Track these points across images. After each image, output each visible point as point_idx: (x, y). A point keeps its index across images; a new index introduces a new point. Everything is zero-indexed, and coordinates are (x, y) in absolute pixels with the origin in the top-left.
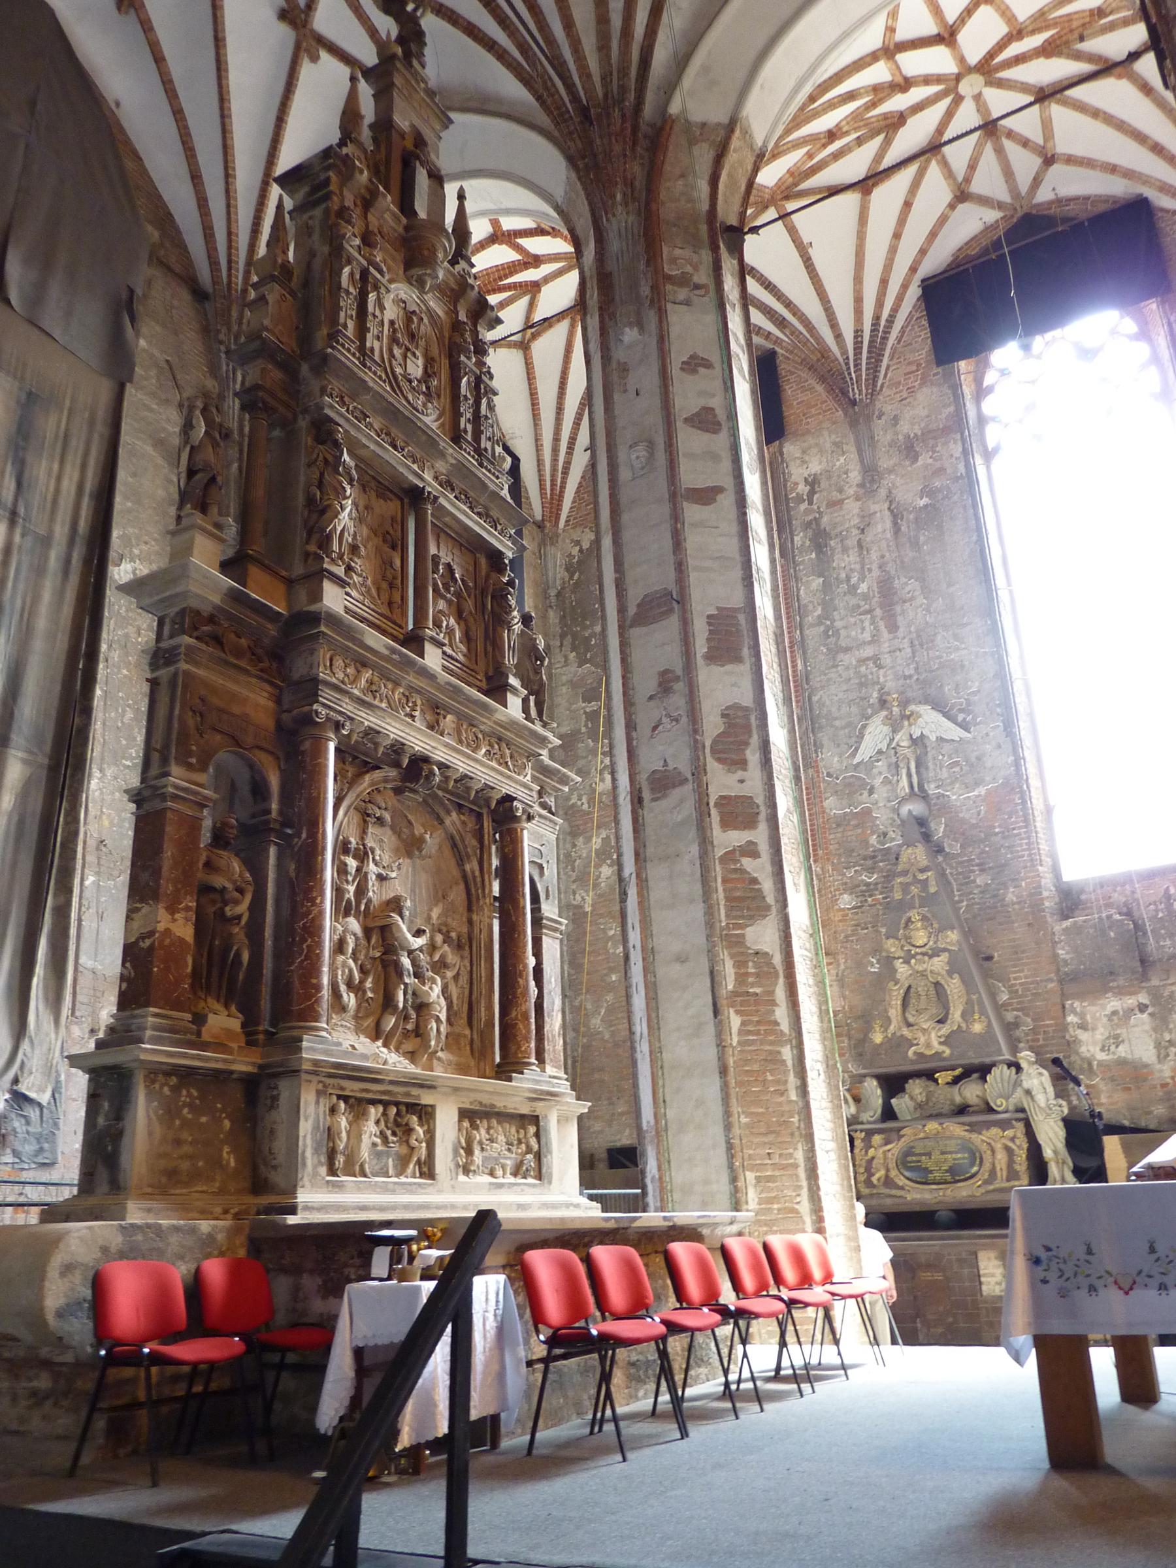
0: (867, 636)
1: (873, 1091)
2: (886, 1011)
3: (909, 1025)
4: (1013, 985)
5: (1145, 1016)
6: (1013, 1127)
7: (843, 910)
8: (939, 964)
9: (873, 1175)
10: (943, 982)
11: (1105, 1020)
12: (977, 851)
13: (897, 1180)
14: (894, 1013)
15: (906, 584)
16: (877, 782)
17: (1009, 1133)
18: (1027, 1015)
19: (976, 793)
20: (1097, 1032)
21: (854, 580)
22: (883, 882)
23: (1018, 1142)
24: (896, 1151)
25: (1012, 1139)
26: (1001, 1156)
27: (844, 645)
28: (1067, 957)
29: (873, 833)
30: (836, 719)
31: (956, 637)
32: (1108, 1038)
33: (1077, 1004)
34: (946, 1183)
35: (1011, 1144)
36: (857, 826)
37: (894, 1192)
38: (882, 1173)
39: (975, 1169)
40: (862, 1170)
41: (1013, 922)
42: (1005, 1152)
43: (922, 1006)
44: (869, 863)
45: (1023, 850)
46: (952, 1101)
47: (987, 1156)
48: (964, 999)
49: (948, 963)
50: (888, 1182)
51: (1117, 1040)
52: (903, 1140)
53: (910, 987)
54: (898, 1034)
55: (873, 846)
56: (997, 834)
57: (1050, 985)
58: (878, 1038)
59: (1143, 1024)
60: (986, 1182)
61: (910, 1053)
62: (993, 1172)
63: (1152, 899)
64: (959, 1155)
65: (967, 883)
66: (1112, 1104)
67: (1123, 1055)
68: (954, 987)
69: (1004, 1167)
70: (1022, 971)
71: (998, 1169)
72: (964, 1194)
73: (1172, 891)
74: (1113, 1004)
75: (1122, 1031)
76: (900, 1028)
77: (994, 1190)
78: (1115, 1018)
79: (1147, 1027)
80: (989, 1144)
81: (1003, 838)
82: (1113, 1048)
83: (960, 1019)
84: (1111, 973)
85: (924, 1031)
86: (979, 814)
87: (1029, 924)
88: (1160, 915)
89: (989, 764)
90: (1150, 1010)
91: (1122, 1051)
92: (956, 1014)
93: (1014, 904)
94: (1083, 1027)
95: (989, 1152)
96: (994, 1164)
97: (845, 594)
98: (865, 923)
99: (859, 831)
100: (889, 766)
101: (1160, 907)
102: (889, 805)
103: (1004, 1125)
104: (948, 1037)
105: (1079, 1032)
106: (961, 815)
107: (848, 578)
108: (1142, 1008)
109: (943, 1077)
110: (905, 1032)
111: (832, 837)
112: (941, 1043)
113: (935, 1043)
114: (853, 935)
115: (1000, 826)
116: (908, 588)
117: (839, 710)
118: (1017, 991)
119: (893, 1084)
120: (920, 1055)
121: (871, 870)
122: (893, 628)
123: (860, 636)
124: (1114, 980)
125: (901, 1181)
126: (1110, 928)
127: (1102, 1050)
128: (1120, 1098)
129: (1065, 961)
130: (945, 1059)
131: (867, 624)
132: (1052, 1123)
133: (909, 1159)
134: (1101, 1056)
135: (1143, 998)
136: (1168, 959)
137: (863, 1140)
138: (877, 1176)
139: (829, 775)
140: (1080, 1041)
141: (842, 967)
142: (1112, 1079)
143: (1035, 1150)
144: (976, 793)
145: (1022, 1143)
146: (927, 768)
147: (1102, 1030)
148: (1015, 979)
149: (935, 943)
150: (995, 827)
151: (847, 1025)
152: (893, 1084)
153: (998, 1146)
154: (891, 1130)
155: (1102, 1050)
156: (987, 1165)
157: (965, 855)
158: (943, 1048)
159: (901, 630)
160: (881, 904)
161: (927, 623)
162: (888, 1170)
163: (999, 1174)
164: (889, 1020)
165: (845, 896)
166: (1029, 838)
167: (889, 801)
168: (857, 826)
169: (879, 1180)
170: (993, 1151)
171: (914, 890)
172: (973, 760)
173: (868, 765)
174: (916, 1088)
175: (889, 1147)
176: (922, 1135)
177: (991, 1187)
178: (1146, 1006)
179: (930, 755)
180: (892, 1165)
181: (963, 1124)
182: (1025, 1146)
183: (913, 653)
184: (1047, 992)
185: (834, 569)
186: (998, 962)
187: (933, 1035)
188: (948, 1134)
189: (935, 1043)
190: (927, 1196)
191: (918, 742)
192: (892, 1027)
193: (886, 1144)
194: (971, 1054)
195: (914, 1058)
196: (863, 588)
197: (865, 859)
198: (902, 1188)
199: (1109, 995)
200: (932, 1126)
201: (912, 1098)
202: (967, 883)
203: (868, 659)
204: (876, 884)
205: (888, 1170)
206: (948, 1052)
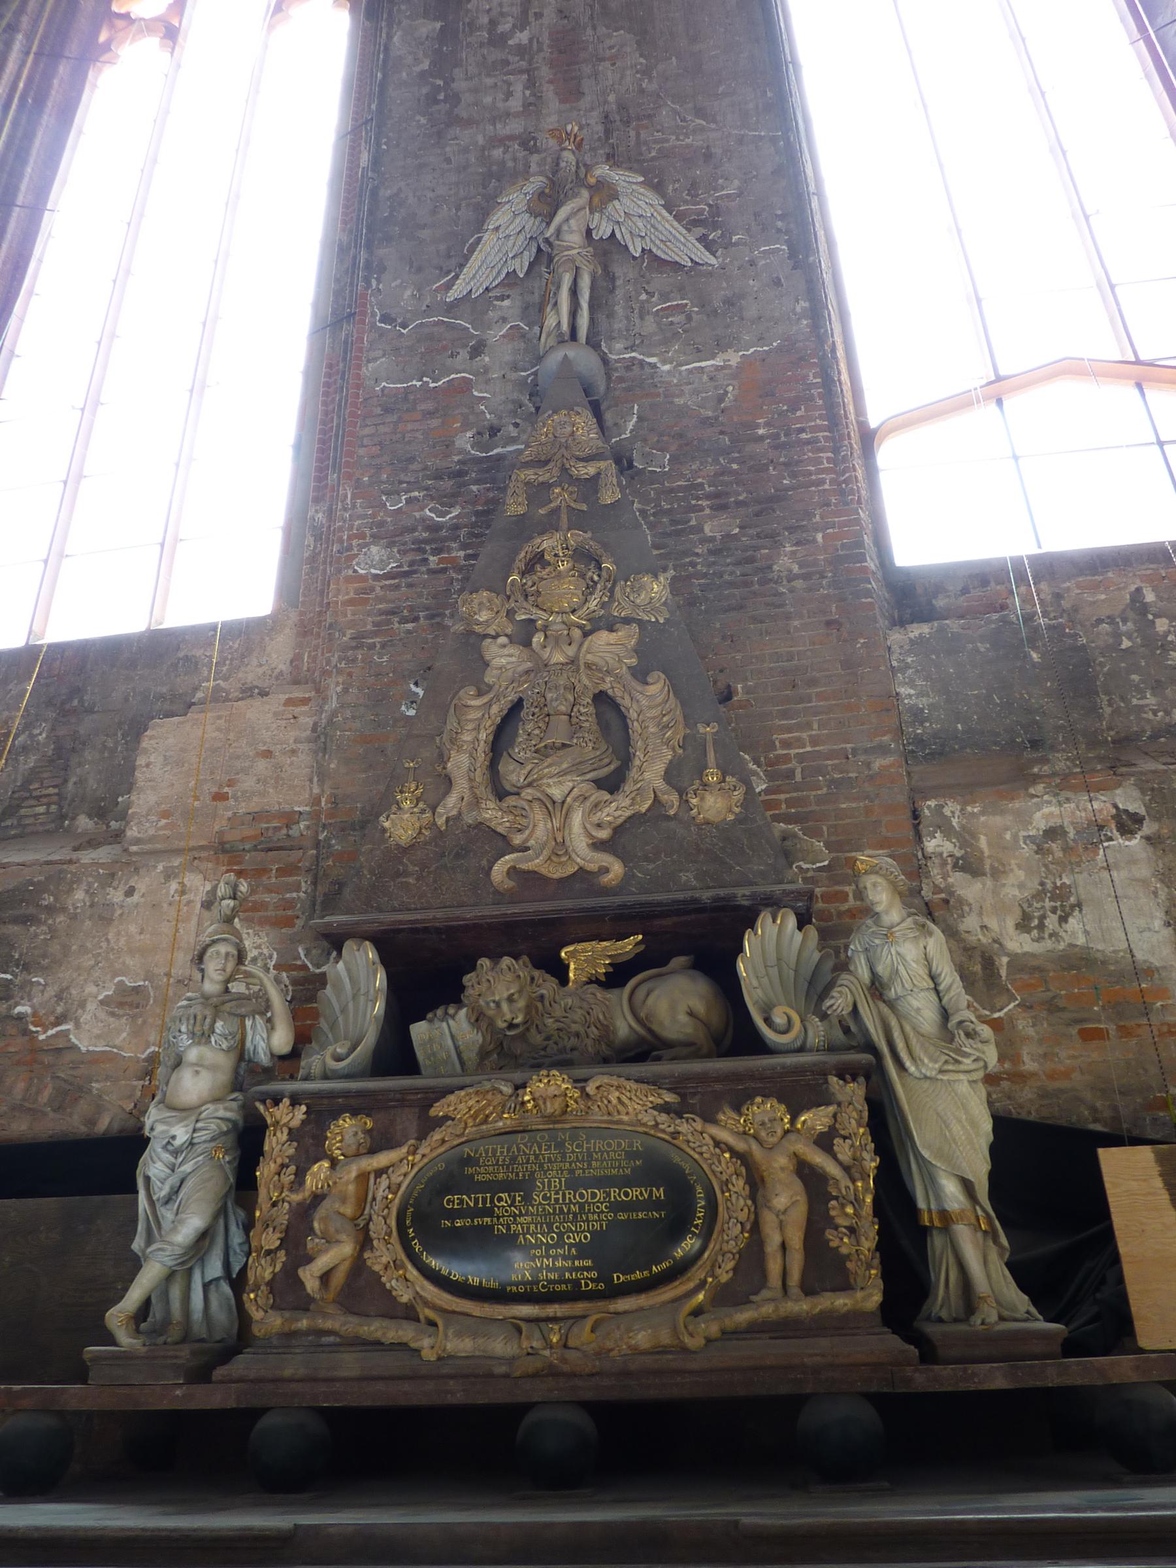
0: (515, 104)
1: (360, 983)
2: (442, 758)
3: (501, 794)
4: (780, 759)
5: (1135, 842)
7: (363, 578)
9: (309, 1260)
11: (1027, 850)
12: (711, 469)
13: (391, 1282)
14: (465, 762)
15: (610, 36)
16: (496, 334)
17: (815, 1119)
18: (815, 833)
19: (718, 362)
20: (1011, 880)
21: (505, 27)
22: (473, 525)
23: (844, 1150)
24: (403, 1177)
25: (825, 1142)
26: (787, 1198)
27: (464, 115)
28: (923, 702)
29: (466, 426)
30: (424, 227)
31: (699, 112)
32: (1039, 896)
33: (951, 808)
34: (575, 1294)
35: (818, 1158)
36: (431, 414)
37: (374, 1329)
38: (346, 1249)
39: (689, 1244)
40: (271, 1240)
41: (788, 617)
42: (798, 1185)
43: (557, 737)
44: (447, 484)
45: (823, 471)
46: (606, 1031)
47: (735, 1201)
48: (677, 734)
49: (636, 651)
50: (360, 1289)
51: (1066, 904)
52: (437, 1136)
53: (518, 705)
54: (469, 819)
55: (462, 451)
56: (761, 438)
57: (878, 763)
58: (402, 825)
59: (1132, 861)
60: (726, 1297)
61: (499, 869)
62: (752, 1256)
63: (1104, 612)
64: (634, 1193)
65: (678, 533)
66: (1052, 1076)
67: (1081, 940)
68: (649, 704)
69: (796, 1240)
70: (809, 726)
71: (773, 1240)
72: (642, 1338)
73: (1150, 597)
74: (1046, 811)
75: (1081, 882)
76: (476, 802)
78: (1055, 847)
79: (1144, 871)
80: (742, 1158)
81: (776, 447)
82: (1051, 922)
83: (659, 784)
84: (1035, 744)
85: (551, 806)
86: (721, 399)
87: (829, 623)
88: (1126, 644)
89: (751, 311)
90: (1149, 828)
91: (1076, 931)
92: (650, 771)
93: (791, 578)
94: (969, 865)
95: (739, 1184)
96: (756, 1228)
97: (482, 45)
98: (411, 609)
99: (435, 423)
100: (526, 308)
101: (1123, 628)
102: (514, 376)
103: (800, 1091)
104: (618, 830)
105: (957, 879)
106: (679, 401)
107: (493, 23)
108: (1127, 823)
109: (584, 958)
111: (367, 431)
112: (598, 846)
113: (579, 843)
114: (375, 634)
115: (767, 424)
116: (609, 42)
117: (434, 212)
118: (790, 774)
119: (425, 974)
120: (527, 879)
121: (446, 500)
122: (571, 93)
123: (500, 105)
124: (1044, 761)
125: (407, 1285)
126: (1032, 642)
127: (1023, 925)
128: (1073, 1056)
129: (918, 715)
130: (606, 891)
131: (518, 88)
132: (963, 1088)
133: (452, 1201)
134: (1020, 943)
135: (1129, 799)
136: (1155, 737)
137: (293, 1135)
138: (323, 1262)
139: (385, 319)
140: (961, 902)
141: (334, 704)
142: (1052, 1007)
144: (718, 362)
146: (611, 315)
147: (1021, 874)
148: (786, 744)
149: (603, 605)
150: (758, 426)
151: (317, 845)
152: (425, 974)
153: (778, 1165)
154: (401, 1099)
155: (1023, 925)
156: (731, 1235)
157: (682, 476)
158: (606, 859)
159: (588, 98)
160: (459, 569)
161: (642, 91)
162: (365, 1242)
163: (774, 1267)
164: (448, 782)
165: (374, 549)
166: (836, 450)
167: (515, 368)
168: (431, 414)
169: (325, 1278)
170: (756, 1183)
171: (561, 497)
172: (717, 303)
173: (477, 306)
174: (500, 985)
175: (382, 1159)
176: (507, 1120)
177: (743, 1316)
178: (1138, 820)
179: (620, 293)
180: (382, 1225)
181: (654, 1082)
183: (608, 133)
184: (871, 778)
185: (468, 11)
186: (744, 705)
187: (577, 818)
188: (597, 1116)
189: (579, 843)
190: (500, 1346)
191: (607, 250)
192: (452, 800)
193: (372, 1151)
194: (687, 877)
195: (509, 884)
196: (523, 37)
197: (438, 477)
198: (409, 1314)
199: (1039, 788)
200: (550, 1086)
201: (478, 1018)
202: (678, 533)
203: (511, 138)
204: (456, 527)
205: (365, 1242)
206: (617, 869)
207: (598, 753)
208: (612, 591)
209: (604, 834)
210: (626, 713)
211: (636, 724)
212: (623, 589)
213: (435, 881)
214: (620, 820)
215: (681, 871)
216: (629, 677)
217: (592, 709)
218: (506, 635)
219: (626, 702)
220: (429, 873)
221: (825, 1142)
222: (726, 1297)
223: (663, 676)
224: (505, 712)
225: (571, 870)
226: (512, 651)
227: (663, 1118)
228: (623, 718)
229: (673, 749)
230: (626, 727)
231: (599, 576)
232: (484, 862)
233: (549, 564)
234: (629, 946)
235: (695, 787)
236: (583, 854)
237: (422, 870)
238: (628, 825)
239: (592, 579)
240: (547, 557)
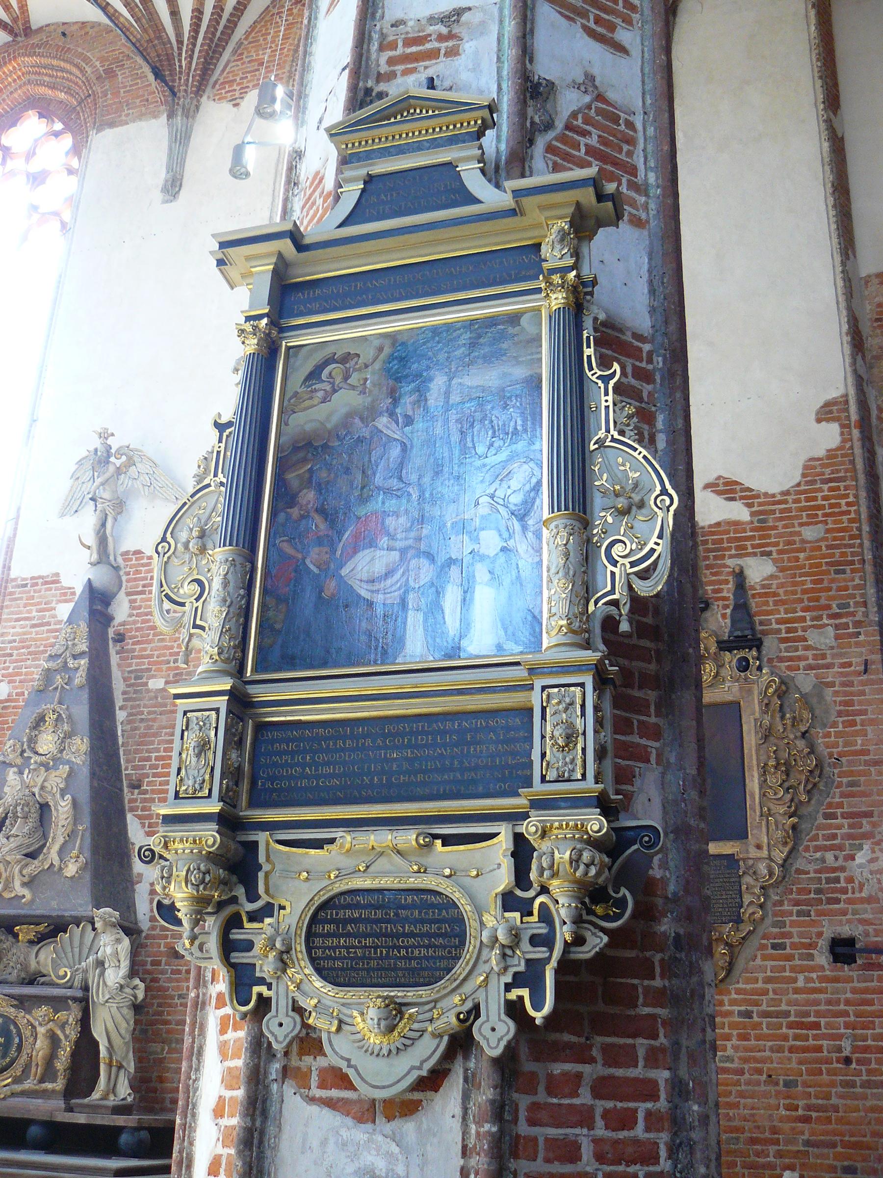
6: (68, 1008)
8: (56, 779)
17: (62, 1015)
35: (59, 1032)
77: (24, 1093)
109: (25, 933)
132: (114, 1010)
143: (86, 1046)
145: (72, 1032)
163: (33, 1070)
177: (18, 1088)
182: (74, 1036)
221: (63, 1027)
222: (17, 1080)
227: (12, 1010)
234: (41, 928)
236: (19, 890)
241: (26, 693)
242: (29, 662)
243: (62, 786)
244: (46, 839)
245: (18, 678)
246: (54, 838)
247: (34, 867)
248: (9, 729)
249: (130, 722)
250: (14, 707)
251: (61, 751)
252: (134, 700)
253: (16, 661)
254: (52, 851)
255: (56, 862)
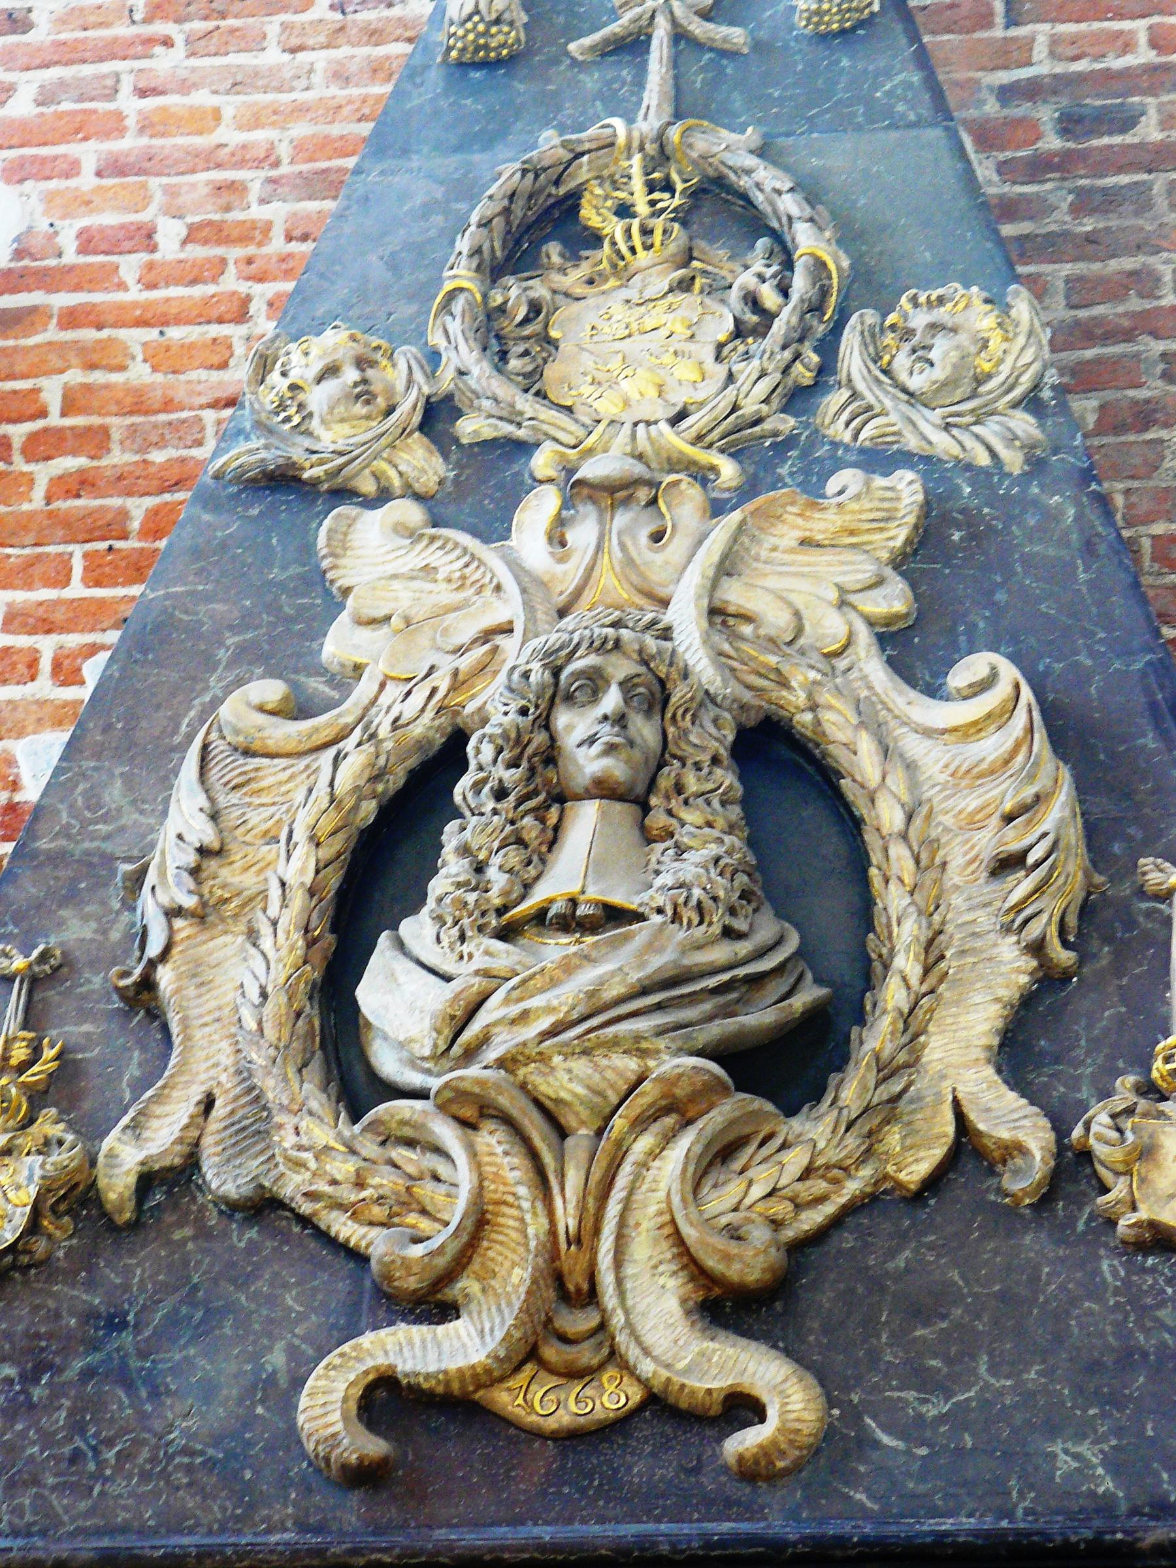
3: (355, 1086)
10: (838, 728)
53: (447, 757)
110: (313, 1151)
112: (724, 1306)
207: (743, 948)
208: (829, 348)
209: (751, 1263)
210: (861, 808)
211: (898, 851)
212: (872, 337)
213: (77, 1427)
214: (813, 1219)
215: (1053, 1431)
216: (872, 668)
217: (726, 778)
218: (418, 497)
219: (862, 762)
220: (56, 1391)
223: (1009, 672)
224: (396, 780)
225: (612, 1397)
226: (434, 556)
228: (851, 825)
229: (1037, 948)
230: (859, 861)
231: (784, 291)
232: (277, 1359)
233: (595, 239)
235: (1119, 1102)
237: (30, 1378)
238: (847, 1240)
239: (752, 301)
240: (589, 215)
241: (169, 234)
242: (164, 62)
243: (893, 599)
244: (867, 973)
245: (89, 153)
246: (932, 954)
247: (801, 1164)
248: (43, 446)
249: (1082, 379)
250: (71, 318)
251: (797, 399)
252: (1091, 246)
253: (68, 54)
254: (937, 1050)
255: (1011, 1120)
